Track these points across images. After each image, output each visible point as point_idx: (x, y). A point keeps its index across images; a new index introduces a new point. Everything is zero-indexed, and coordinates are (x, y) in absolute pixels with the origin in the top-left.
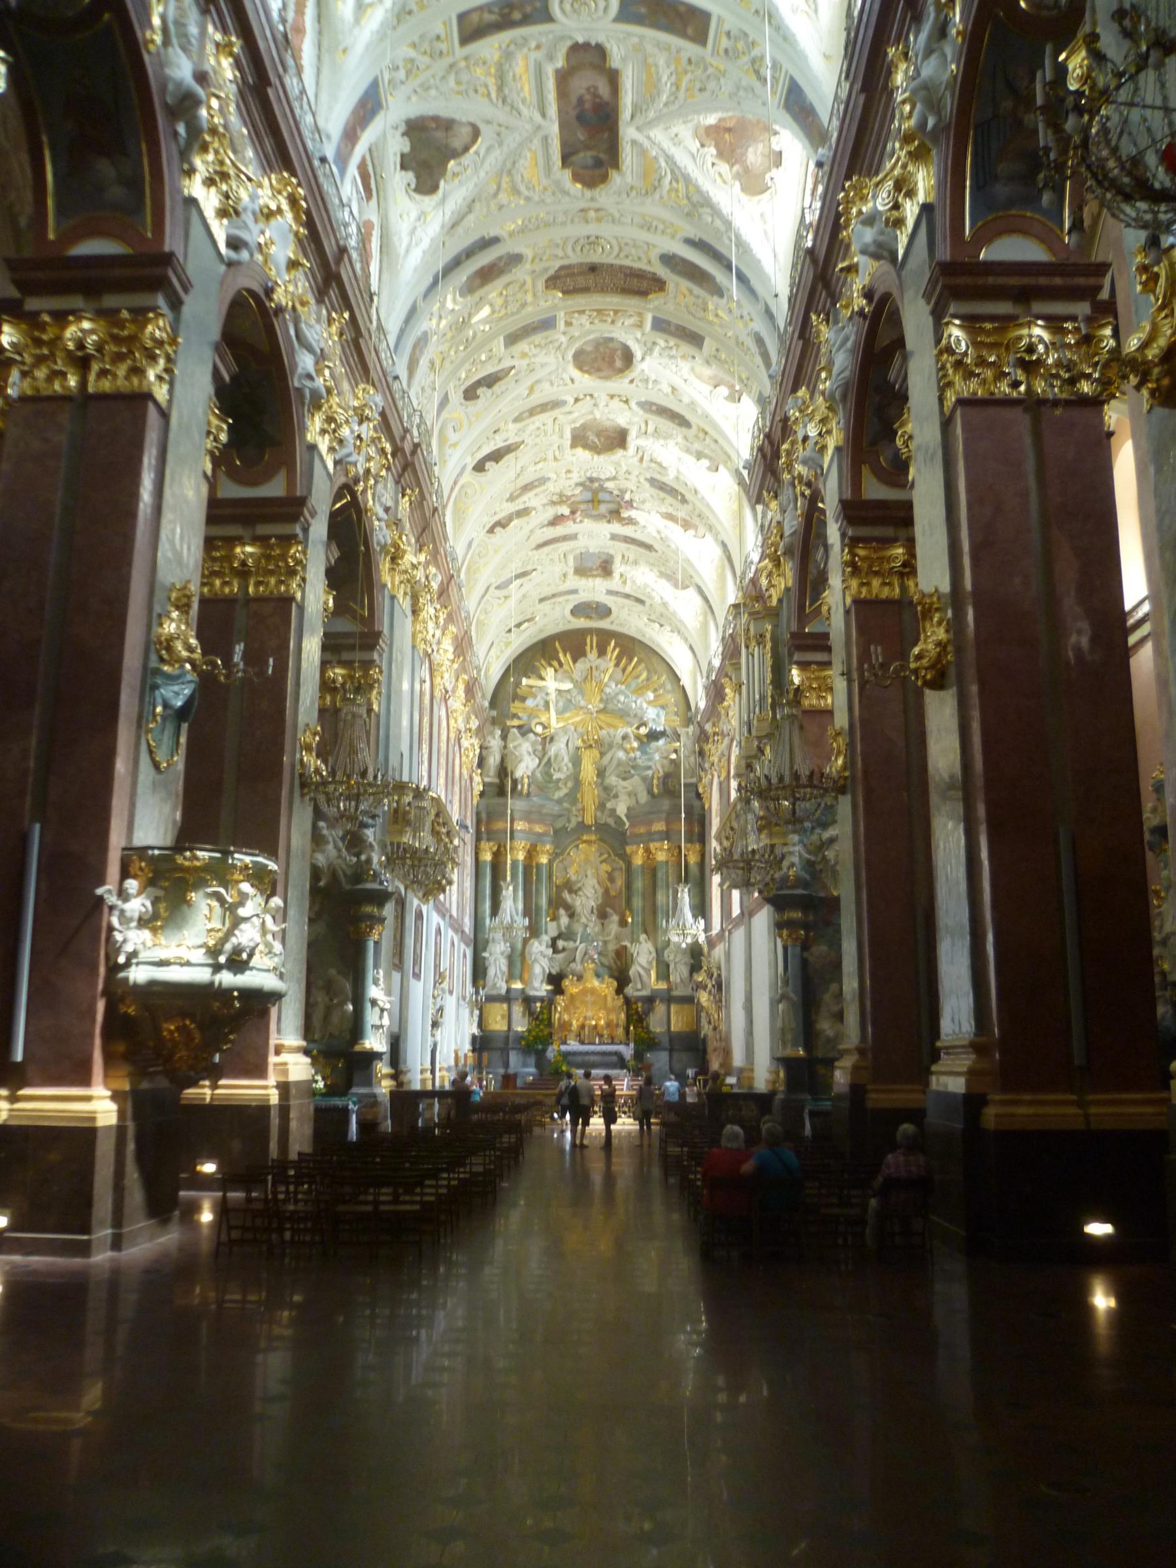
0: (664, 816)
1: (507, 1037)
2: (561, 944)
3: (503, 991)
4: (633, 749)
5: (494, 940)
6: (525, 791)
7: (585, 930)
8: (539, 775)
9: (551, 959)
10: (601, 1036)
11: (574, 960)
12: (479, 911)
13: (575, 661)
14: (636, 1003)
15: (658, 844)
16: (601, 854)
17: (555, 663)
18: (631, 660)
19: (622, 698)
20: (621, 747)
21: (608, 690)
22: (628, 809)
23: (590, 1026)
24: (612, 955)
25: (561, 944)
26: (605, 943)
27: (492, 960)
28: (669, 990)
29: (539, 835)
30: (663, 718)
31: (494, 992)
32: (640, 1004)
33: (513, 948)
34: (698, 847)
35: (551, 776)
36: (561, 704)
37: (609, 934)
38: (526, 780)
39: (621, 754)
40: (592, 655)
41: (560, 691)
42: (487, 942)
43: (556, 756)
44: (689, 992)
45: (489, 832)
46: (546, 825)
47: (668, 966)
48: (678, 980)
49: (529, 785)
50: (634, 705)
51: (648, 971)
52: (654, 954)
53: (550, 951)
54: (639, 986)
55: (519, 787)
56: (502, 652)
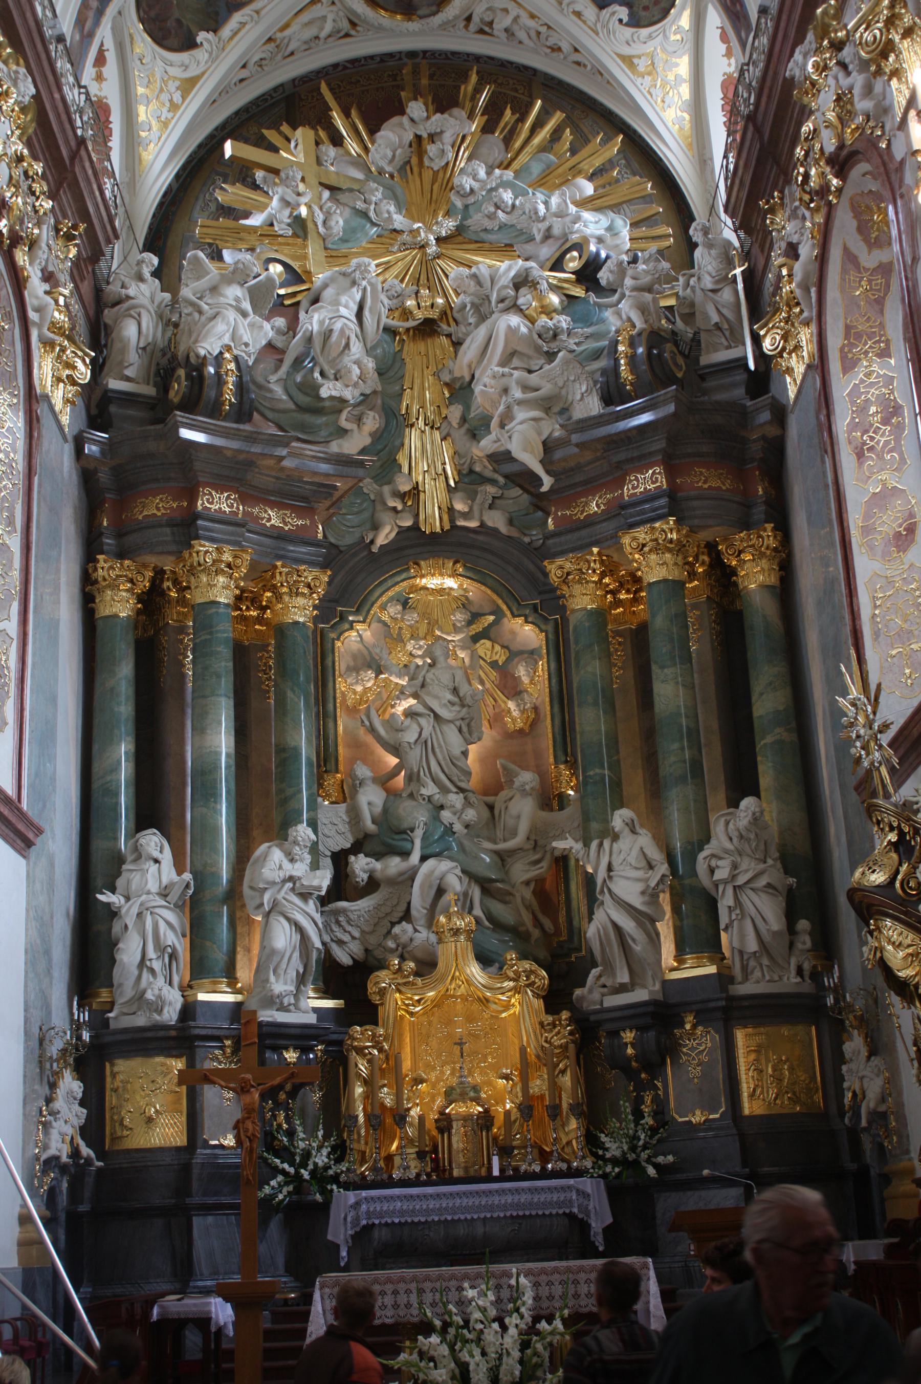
0: (660, 444)
1: (186, 1168)
2: (361, 865)
3: (170, 1015)
4: (548, 311)
5: (138, 854)
6: (229, 395)
7: (436, 818)
8: (278, 391)
9: (332, 919)
10: (505, 1151)
11: (407, 916)
12: (96, 767)
13: (373, 131)
14: (615, 1034)
15: (642, 534)
16: (475, 617)
17: (322, 134)
18: (522, 113)
19: (507, 196)
20: (515, 308)
21: (467, 183)
22: (548, 446)
23: (466, 1118)
24: (528, 893)
25: (361, 865)
26: (502, 857)
27: (129, 913)
28: (724, 979)
29: (279, 536)
30: (625, 232)
31: (140, 1020)
32: (628, 1036)
33: (202, 878)
34: (769, 537)
35: (311, 389)
36: (339, 222)
37: (514, 833)
38: (232, 366)
39: (514, 320)
40: (416, 109)
41: (332, 188)
42: (118, 860)
43: (327, 334)
44: (790, 982)
45: (120, 535)
46: (300, 512)
47: (712, 904)
48: (752, 945)
49: (240, 386)
50: (542, 208)
51: (647, 921)
52: (664, 868)
53: (323, 879)
54: (624, 977)
55: (210, 393)
56: (174, 107)
